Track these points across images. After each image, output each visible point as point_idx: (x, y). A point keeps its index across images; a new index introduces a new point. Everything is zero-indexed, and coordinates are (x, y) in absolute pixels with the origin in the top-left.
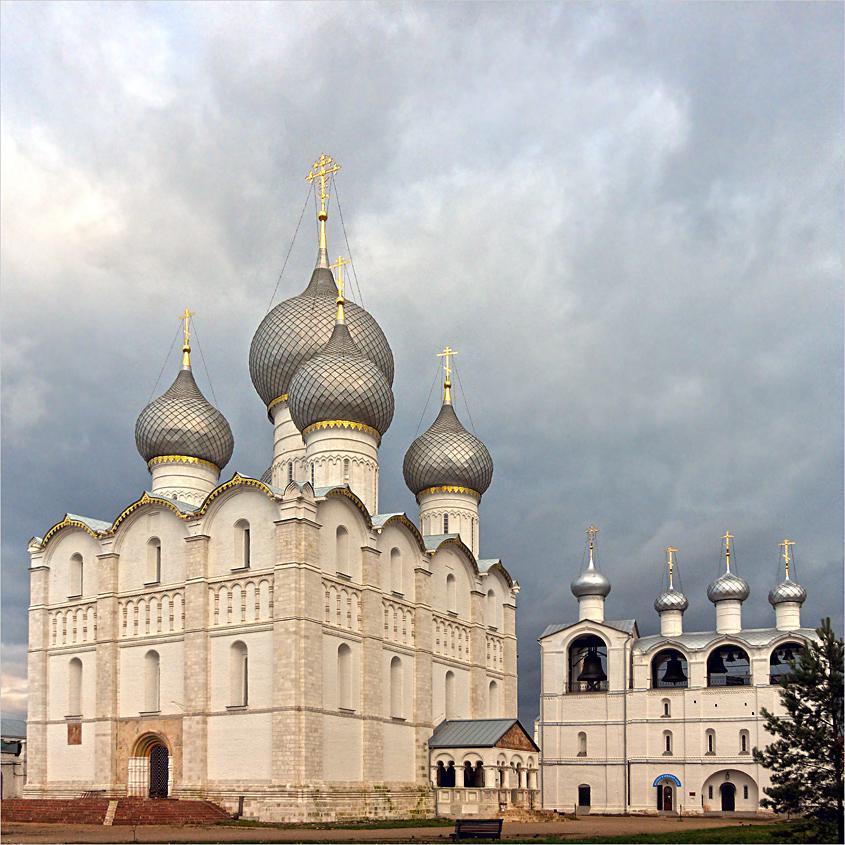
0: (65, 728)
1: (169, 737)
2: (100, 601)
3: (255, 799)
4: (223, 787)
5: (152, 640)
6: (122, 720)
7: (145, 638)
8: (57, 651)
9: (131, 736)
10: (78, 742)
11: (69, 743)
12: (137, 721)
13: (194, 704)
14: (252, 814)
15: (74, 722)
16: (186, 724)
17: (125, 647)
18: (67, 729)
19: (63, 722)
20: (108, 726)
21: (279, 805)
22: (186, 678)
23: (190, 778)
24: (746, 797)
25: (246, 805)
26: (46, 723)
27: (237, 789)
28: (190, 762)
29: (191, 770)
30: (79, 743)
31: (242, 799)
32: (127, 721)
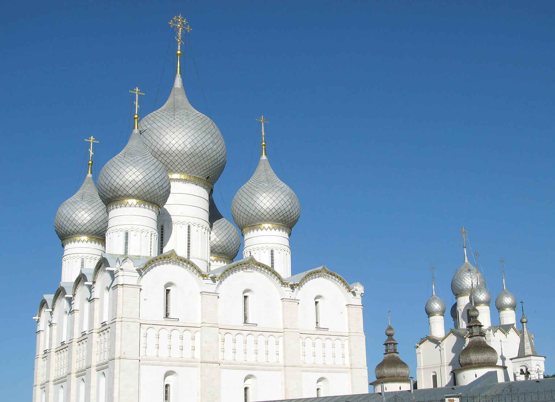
7: (244, 364)
17: (226, 368)
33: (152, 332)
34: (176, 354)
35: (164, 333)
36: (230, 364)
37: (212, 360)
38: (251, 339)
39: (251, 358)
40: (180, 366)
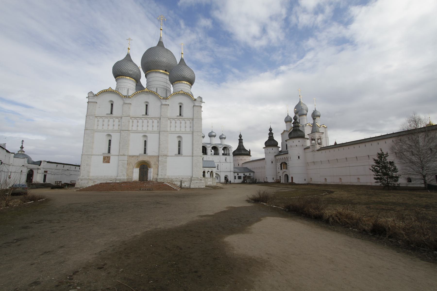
0: (102, 158)
1: (151, 162)
2: (123, 117)
3: (186, 181)
4: (173, 178)
5: (145, 132)
6: (130, 156)
7: (142, 131)
8: (99, 131)
9: (135, 161)
10: (109, 162)
11: (104, 162)
12: (137, 156)
13: (163, 152)
14: (185, 186)
15: (107, 155)
16: (160, 159)
17: (133, 133)
19: (101, 155)
20: (126, 158)
21: (197, 183)
22: (159, 145)
23: (161, 175)
24: (217, 179)
25: (183, 183)
26: (92, 155)
27: (179, 178)
28: (162, 170)
30: (109, 162)
32: (133, 156)
33: (101, 120)
34: (111, 128)
35: (106, 120)
36: (135, 131)
38: (145, 121)
39: (145, 129)
40: (112, 132)
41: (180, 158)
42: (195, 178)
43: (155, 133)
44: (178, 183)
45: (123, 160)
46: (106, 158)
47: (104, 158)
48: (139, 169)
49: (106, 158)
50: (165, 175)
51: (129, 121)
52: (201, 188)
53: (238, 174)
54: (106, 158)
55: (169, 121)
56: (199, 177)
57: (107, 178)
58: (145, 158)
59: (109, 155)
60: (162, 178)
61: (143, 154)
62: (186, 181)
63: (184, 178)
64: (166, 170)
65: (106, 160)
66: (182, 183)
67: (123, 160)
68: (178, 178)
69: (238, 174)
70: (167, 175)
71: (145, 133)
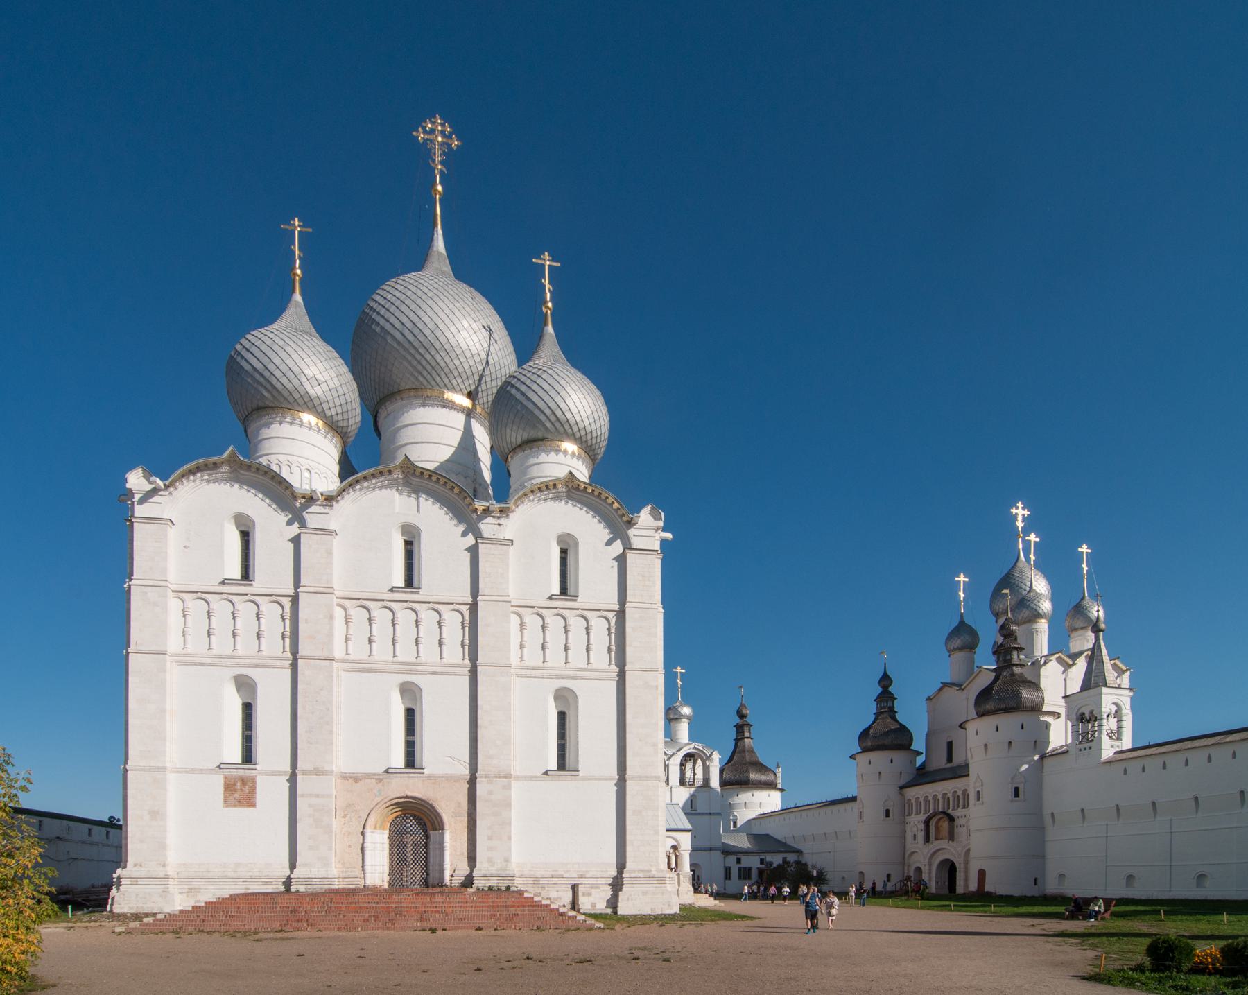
0: (218, 781)
7: (393, 663)
10: (251, 803)
15: (241, 772)
18: (222, 783)
21: (645, 893)
23: (490, 860)
25: (584, 895)
27: (565, 875)
28: (490, 838)
29: (490, 849)
30: (251, 803)
31: (574, 888)
36: (360, 662)
37: (318, 654)
41: (564, 786)
42: (634, 871)
43: (455, 674)
44: (561, 894)
45: (317, 796)
46: (239, 784)
47: (229, 787)
48: (387, 833)
49: (235, 785)
50: (507, 860)
51: (331, 617)
52: (665, 915)
53: (739, 861)
54: (239, 784)
55: (515, 620)
56: (653, 869)
57: (250, 874)
58: (413, 787)
59: (248, 773)
60: (494, 872)
61: (403, 767)
62: (598, 888)
63: (587, 875)
64: (509, 838)
65: (236, 795)
66: (580, 894)
67: (317, 796)
68: (561, 873)
69: (739, 861)
70: (515, 859)
71: (410, 673)
